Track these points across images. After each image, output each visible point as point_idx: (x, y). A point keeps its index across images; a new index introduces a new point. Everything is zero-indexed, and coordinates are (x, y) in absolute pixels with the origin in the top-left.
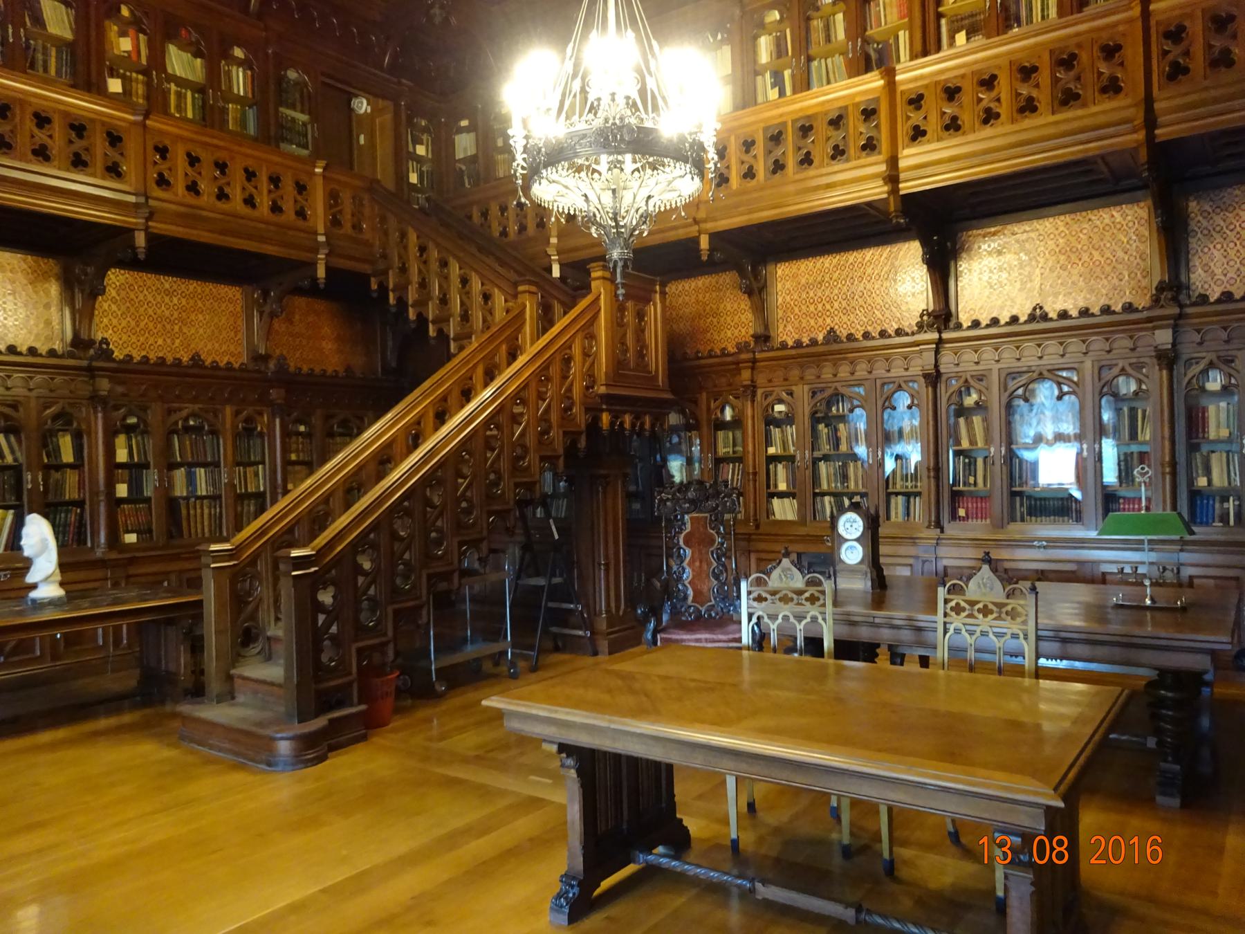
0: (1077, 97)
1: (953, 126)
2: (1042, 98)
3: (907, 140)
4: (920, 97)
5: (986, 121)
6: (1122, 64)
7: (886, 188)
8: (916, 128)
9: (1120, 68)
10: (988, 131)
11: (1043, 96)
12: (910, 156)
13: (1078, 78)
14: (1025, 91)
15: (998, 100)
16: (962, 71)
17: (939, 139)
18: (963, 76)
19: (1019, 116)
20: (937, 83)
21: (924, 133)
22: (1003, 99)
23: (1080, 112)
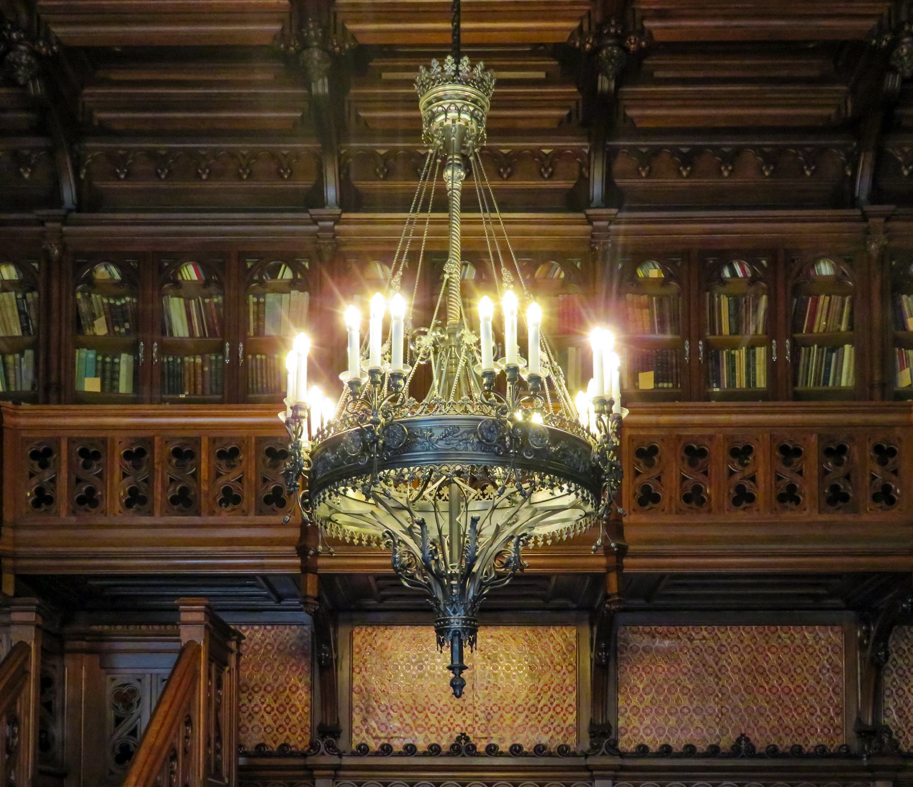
0: (845, 498)
1: (694, 498)
2: (806, 489)
3: (634, 502)
4: (653, 450)
5: (736, 502)
6: (895, 472)
7: (603, 561)
8: (646, 489)
9: (894, 477)
10: (740, 515)
11: (809, 488)
12: (640, 526)
13: (848, 477)
14: (788, 477)
15: (753, 479)
16: (710, 431)
17: (679, 512)
18: (711, 438)
19: (778, 506)
20: (679, 438)
21: (656, 499)
22: (760, 478)
23: (850, 518)
